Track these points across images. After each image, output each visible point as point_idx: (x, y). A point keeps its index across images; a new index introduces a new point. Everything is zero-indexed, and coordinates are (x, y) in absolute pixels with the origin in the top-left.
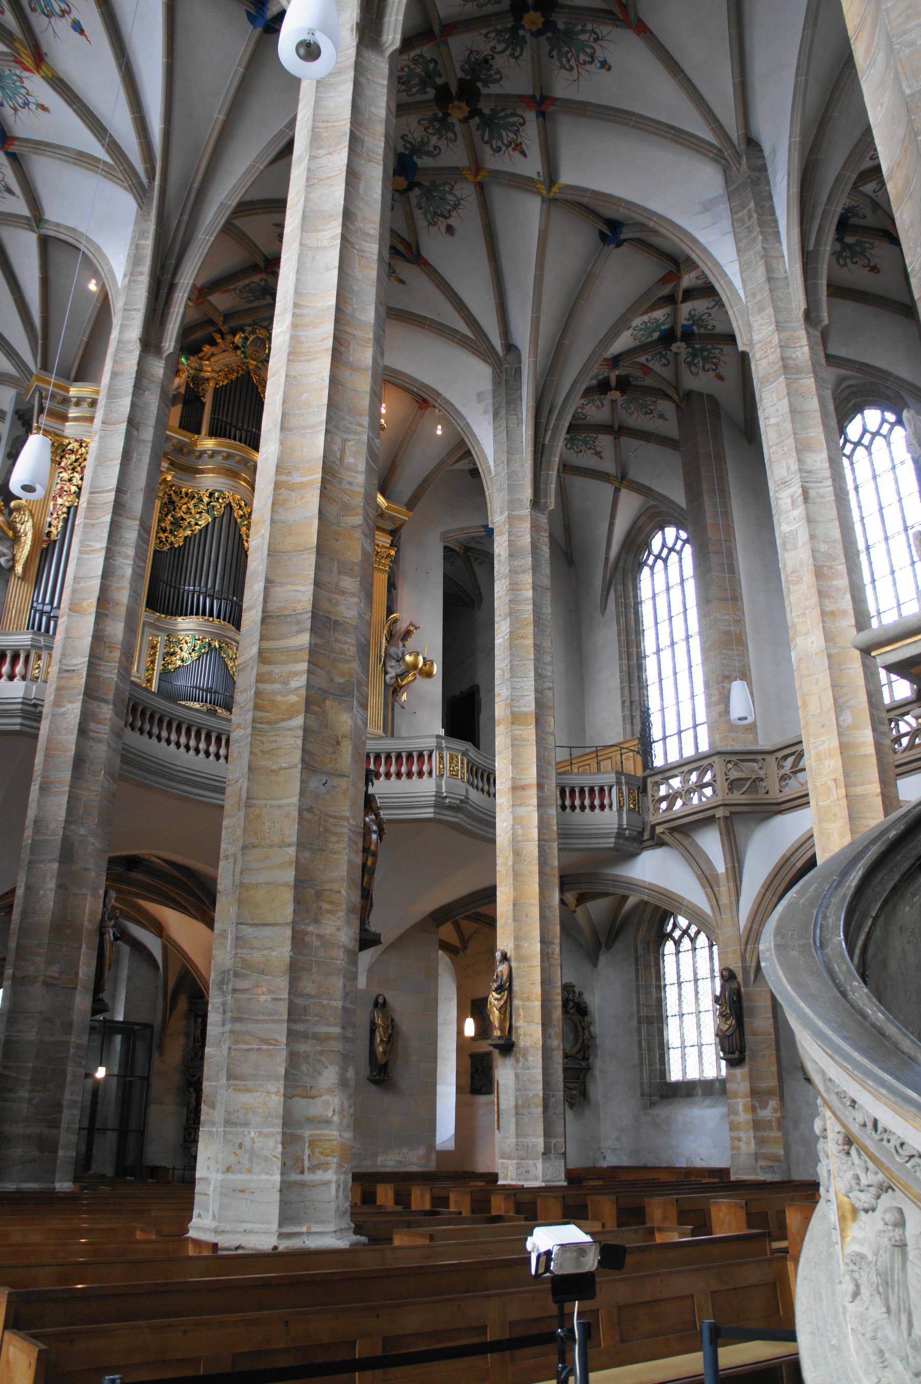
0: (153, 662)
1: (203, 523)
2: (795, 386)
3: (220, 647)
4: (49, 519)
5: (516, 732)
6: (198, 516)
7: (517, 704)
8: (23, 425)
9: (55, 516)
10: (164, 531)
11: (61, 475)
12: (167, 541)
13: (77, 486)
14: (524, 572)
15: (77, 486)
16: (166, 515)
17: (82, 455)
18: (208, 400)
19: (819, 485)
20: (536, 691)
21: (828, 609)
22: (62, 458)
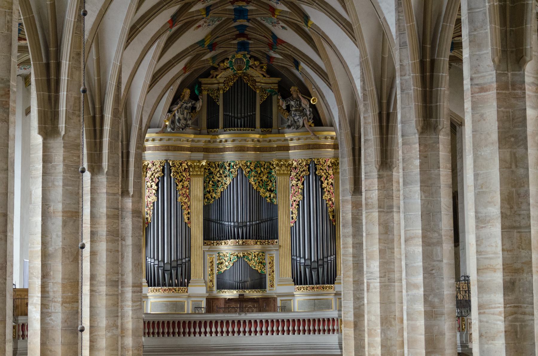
0: (212, 270)
1: (228, 183)
2: (370, 216)
3: (244, 256)
5: (346, 332)
6: (225, 179)
7: (347, 316)
10: (209, 192)
12: (212, 197)
14: (349, 236)
16: (209, 183)
18: (221, 103)
19: (375, 281)
20: (355, 308)
21: (372, 353)
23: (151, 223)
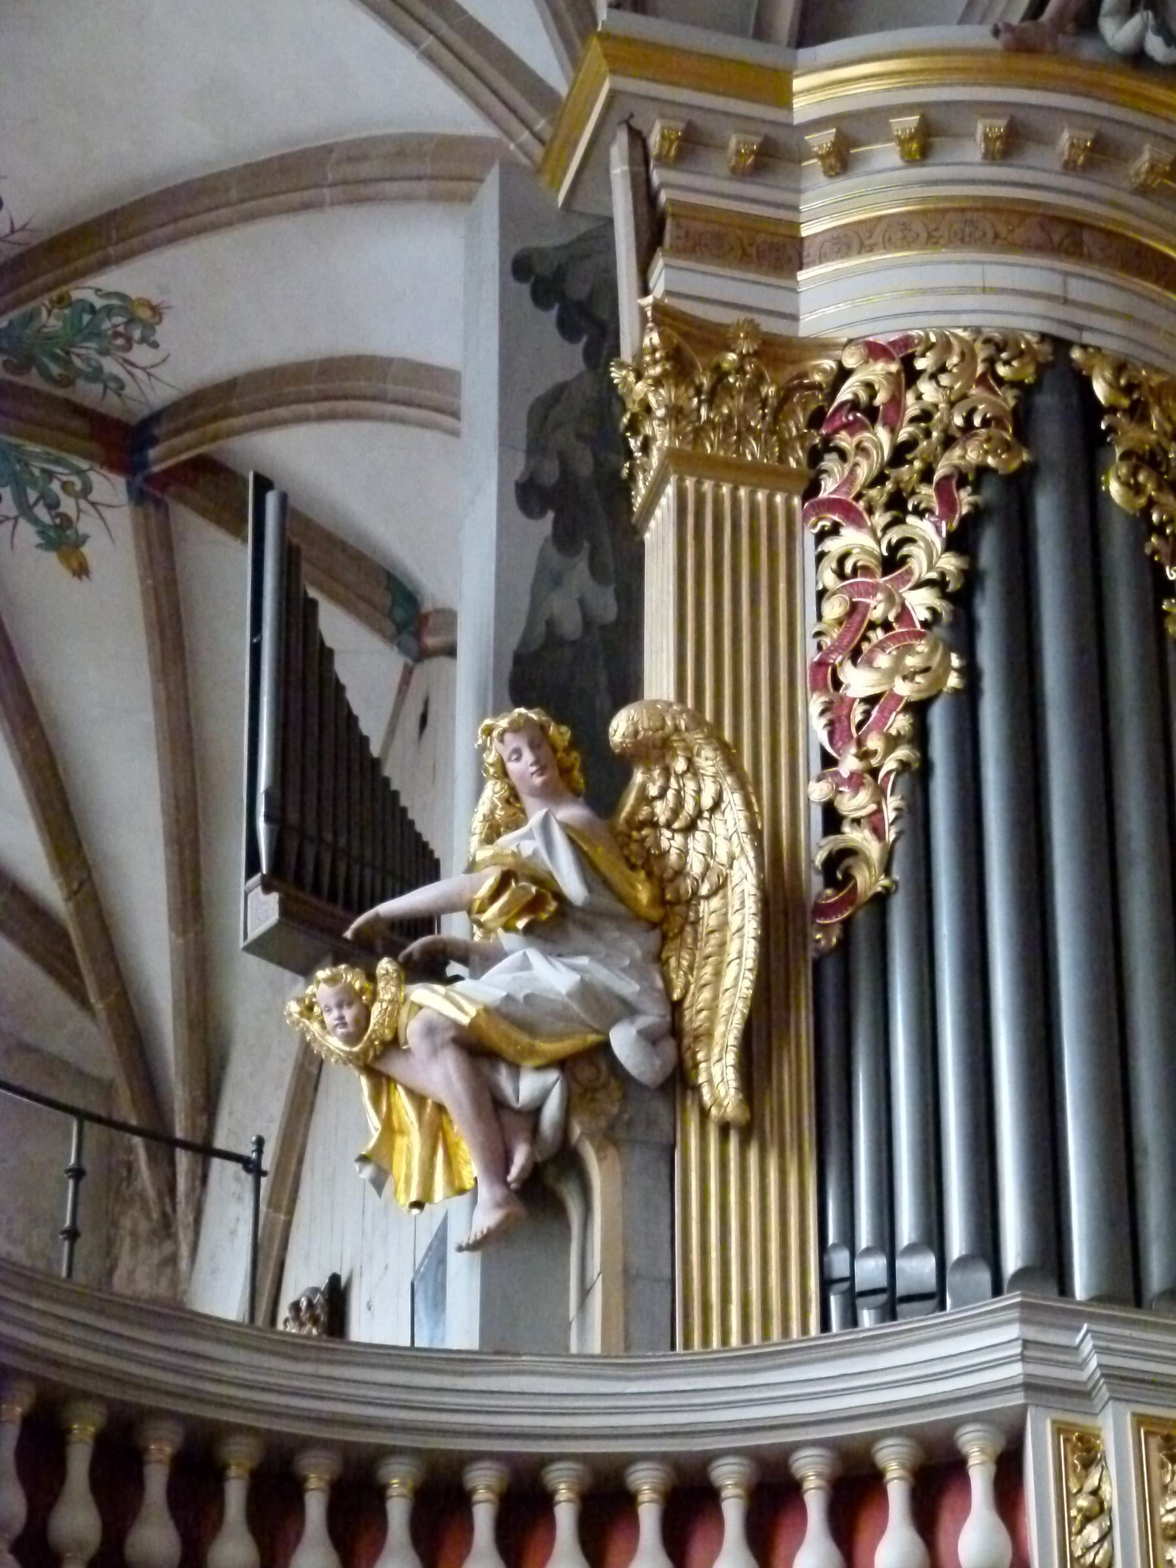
4: (818, 791)
8: (568, 329)
9: (849, 764)
11: (833, 546)
13: (939, 584)
15: (939, 584)
17: (925, 416)
22: (815, 456)
23: (881, 900)
